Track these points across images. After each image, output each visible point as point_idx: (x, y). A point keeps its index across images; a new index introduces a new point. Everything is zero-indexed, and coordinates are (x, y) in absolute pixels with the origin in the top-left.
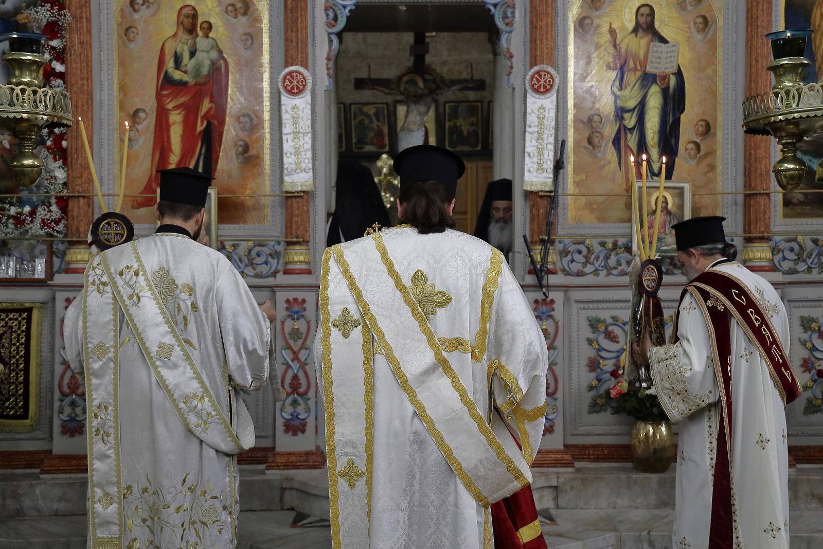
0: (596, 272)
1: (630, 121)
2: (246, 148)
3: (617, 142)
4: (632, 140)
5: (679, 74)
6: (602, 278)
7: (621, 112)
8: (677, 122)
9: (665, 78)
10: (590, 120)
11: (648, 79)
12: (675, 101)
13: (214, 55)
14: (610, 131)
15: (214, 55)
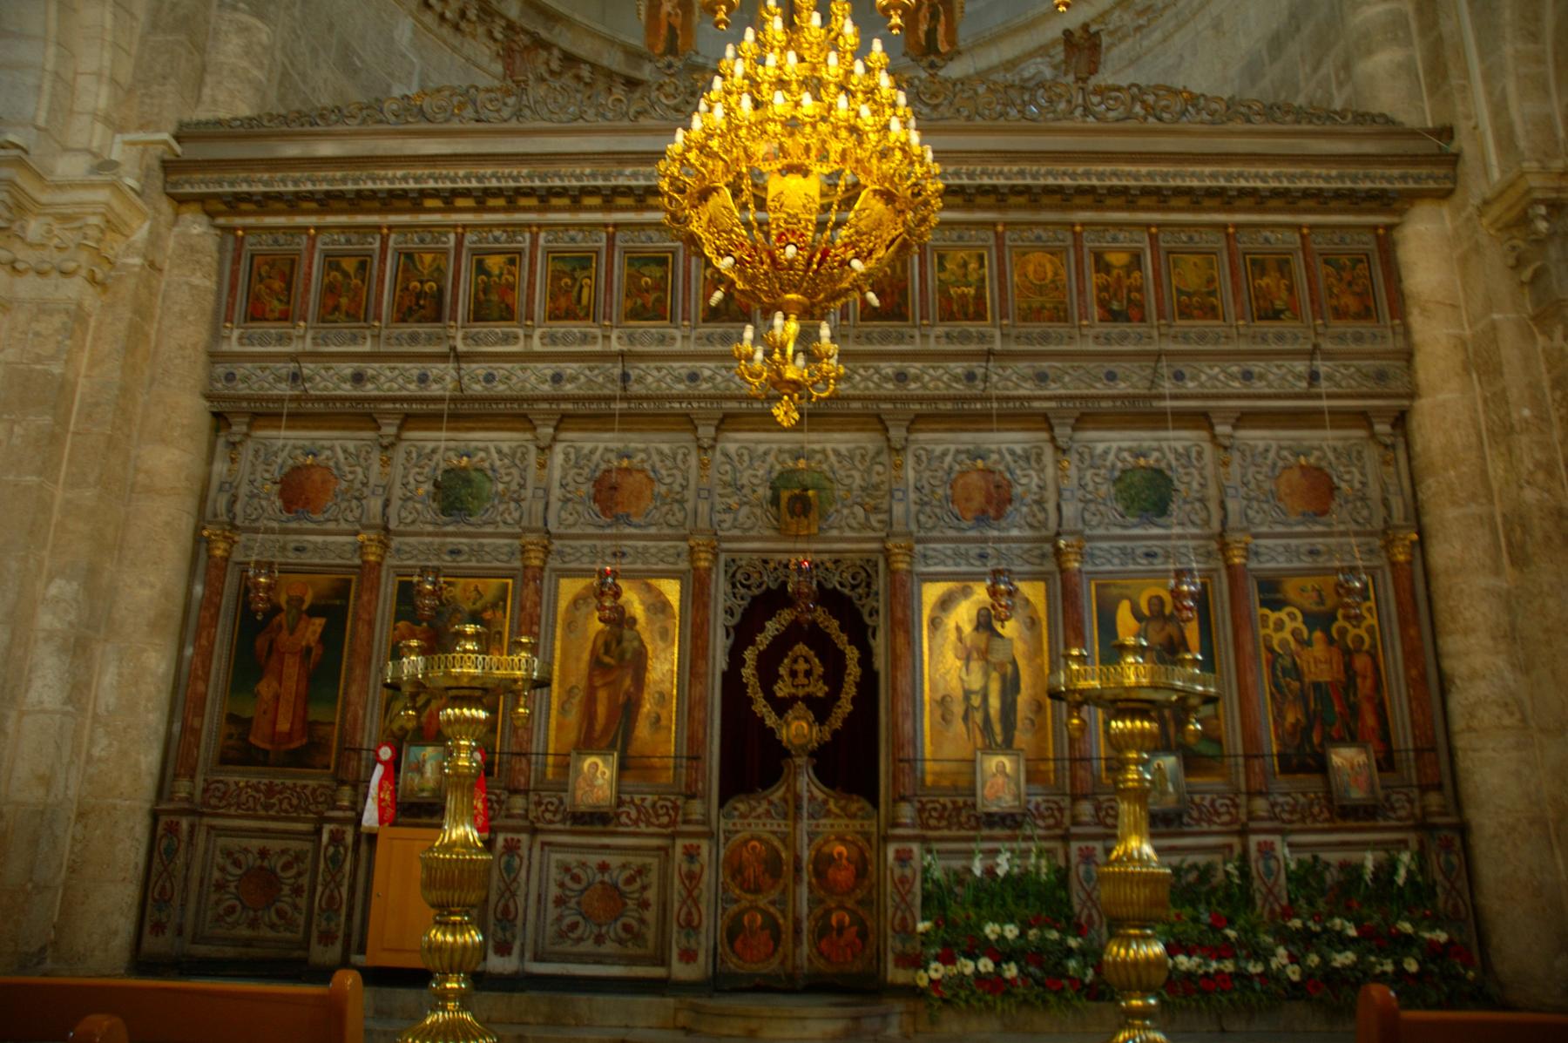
0: (949, 827)
1: (976, 701)
2: (658, 719)
3: (966, 718)
4: (978, 717)
5: (1014, 663)
6: (954, 833)
7: (967, 694)
8: (1014, 701)
9: (1002, 665)
10: (943, 698)
11: (988, 667)
12: (1011, 686)
13: (636, 644)
14: (958, 709)
15: (636, 644)
